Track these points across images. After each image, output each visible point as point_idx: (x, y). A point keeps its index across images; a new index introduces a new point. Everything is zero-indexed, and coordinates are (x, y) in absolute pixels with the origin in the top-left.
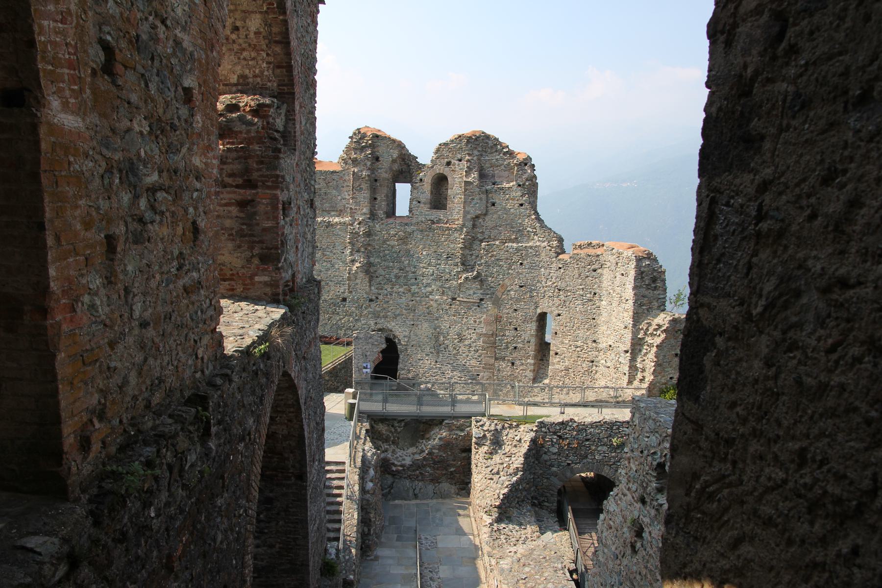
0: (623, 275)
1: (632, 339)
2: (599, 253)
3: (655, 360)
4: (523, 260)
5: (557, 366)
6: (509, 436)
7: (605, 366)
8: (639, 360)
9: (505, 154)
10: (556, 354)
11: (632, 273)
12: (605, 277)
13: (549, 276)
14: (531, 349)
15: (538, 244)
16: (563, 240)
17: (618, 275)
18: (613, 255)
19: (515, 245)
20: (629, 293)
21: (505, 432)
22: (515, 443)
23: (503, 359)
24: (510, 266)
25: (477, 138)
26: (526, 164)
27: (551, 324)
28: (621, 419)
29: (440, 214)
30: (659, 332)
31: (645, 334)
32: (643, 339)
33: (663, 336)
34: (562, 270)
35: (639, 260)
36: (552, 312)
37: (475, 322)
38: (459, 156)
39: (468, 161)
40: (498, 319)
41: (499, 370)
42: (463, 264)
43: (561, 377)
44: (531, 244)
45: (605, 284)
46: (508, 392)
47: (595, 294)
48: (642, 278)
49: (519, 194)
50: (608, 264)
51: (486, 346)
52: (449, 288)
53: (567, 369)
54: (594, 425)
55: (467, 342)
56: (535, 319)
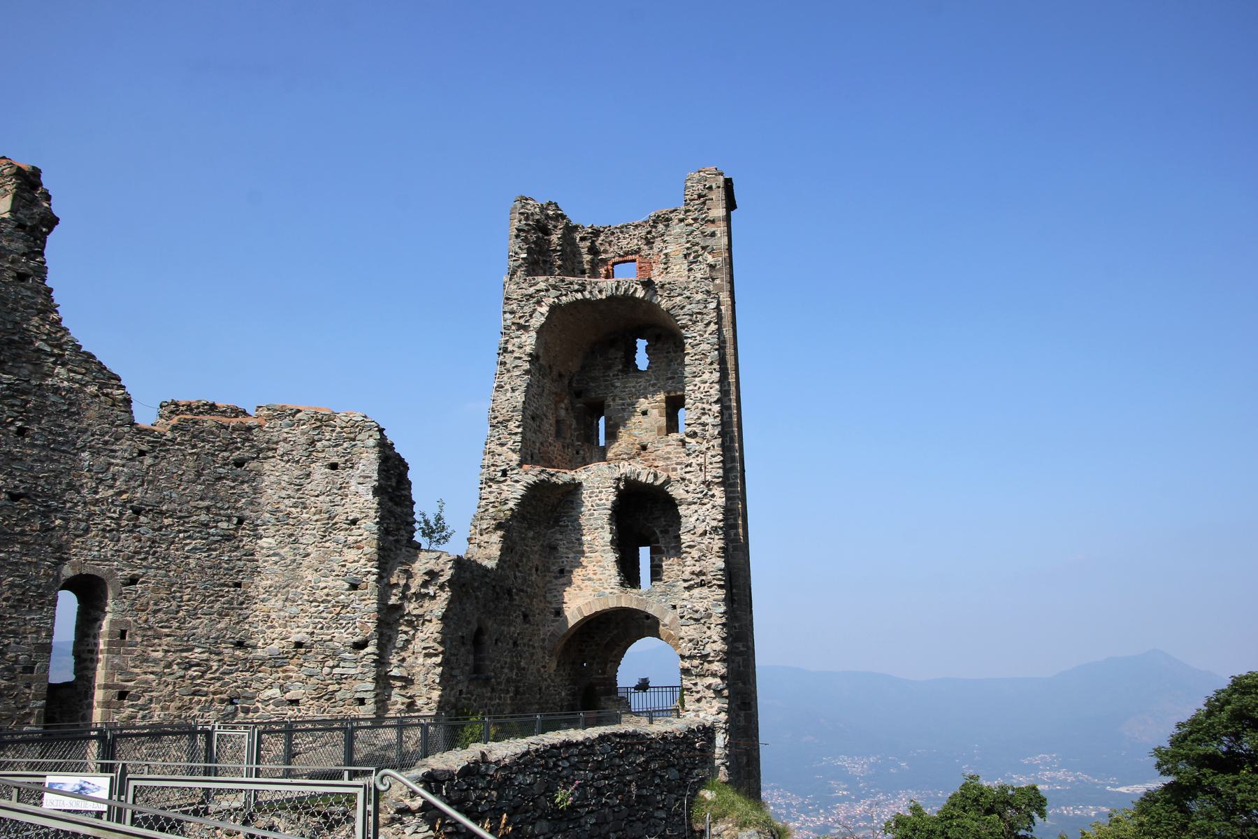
0: (334, 466)
1: (379, 610)
3: (441, 649)
8: (394, 660)
12: (267, 481)
17: (319, 471)
30: (431, 590)
31: (404, 597)
33: (445, 595)
34: (148, 460)
47: (241, 521)
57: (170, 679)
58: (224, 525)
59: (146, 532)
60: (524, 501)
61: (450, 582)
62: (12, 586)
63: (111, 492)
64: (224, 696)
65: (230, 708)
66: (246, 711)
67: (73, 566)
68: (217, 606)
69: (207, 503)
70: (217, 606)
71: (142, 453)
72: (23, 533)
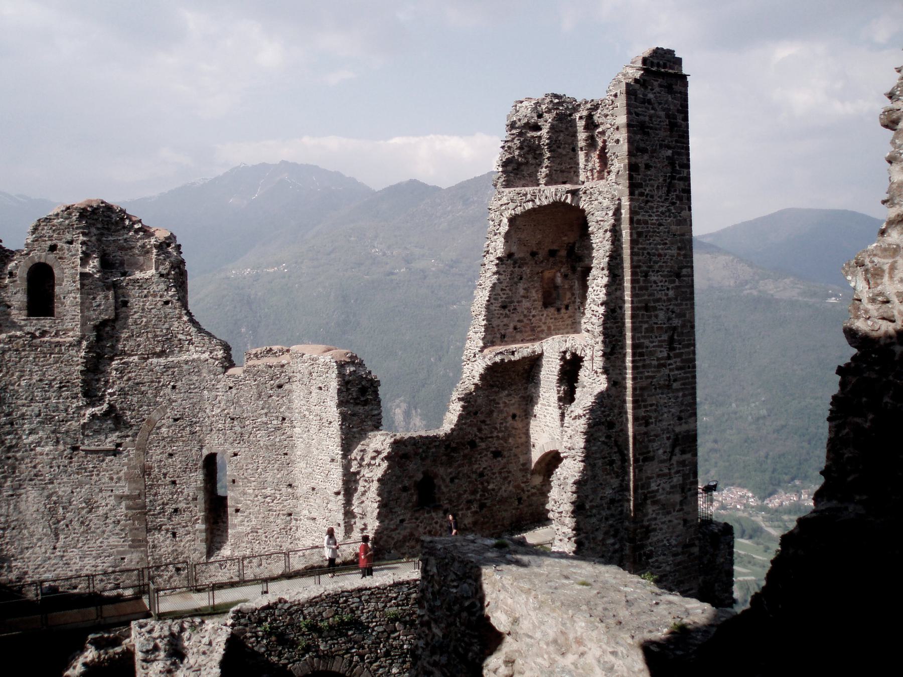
0: (320, 388)
1: (344, 475)
2: (284, 362)
3: (379, 499)
4: (176, 381)
5: (240, 529)
6: (190, 641)
7: (308, 518)
8: (355, 501)
9: (137, 231)
10: (237, 511)
11: (334, 385)
12: (294, 396)
13: (217, 398)
14: (199, 510)
15: (195, 356)
16: (230, 349)
18: (304, 362)
19: (162, 360)
20: (333, 412)
21: (186, 635)
22: (203, 648)
23: (159, 529)
24: (157, 390)
25: (95, 210)
26: (169, 245)
27: (228, 471)
28: (349, 588)
29: (46, 323)
30: (378, 461)
31: (361, 466)
32: (358, 473)
33: (385, 465)
34: (234, 391)
35: (341, 366)
36: (224, 452)
37: (111, 479)
38: (69, 237)
39: (83, 243)
40: (146, 471)
41: (154, 547)
42: (86, 394)
43: (248, 542)
44: (184, 357)
45: (297, 403)
46: (171, 577)
47: (284, 419)
48: (348, 389)
49: (163, 286)
50: (299, 376)
51: (130, 513)
52: (67, 432)
53: (254, 531)
54: (312, 602)
55: (101, 511)
56: (200, 463)
57: (257, 503)
58: (275, 422)
59: (238, 429)
60: (482, 377)
61: (386, 458)
62: (181, 462)
63: (219, 410)
64: (285, 512)
65: (288, 518)
66: (297, 520)
67: (208, 449)
68: (276, 466)
69: (266, 411)
70: (276, 466)
71: (231, 388)
72: (182, 436)
